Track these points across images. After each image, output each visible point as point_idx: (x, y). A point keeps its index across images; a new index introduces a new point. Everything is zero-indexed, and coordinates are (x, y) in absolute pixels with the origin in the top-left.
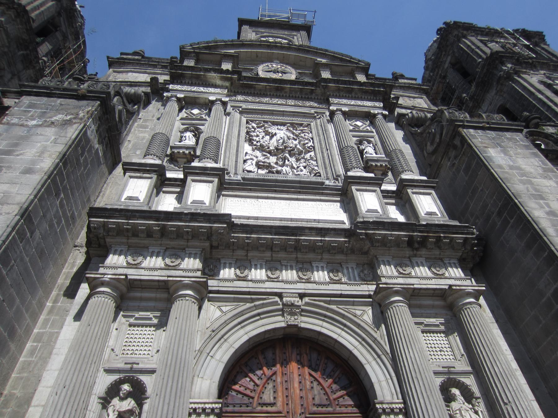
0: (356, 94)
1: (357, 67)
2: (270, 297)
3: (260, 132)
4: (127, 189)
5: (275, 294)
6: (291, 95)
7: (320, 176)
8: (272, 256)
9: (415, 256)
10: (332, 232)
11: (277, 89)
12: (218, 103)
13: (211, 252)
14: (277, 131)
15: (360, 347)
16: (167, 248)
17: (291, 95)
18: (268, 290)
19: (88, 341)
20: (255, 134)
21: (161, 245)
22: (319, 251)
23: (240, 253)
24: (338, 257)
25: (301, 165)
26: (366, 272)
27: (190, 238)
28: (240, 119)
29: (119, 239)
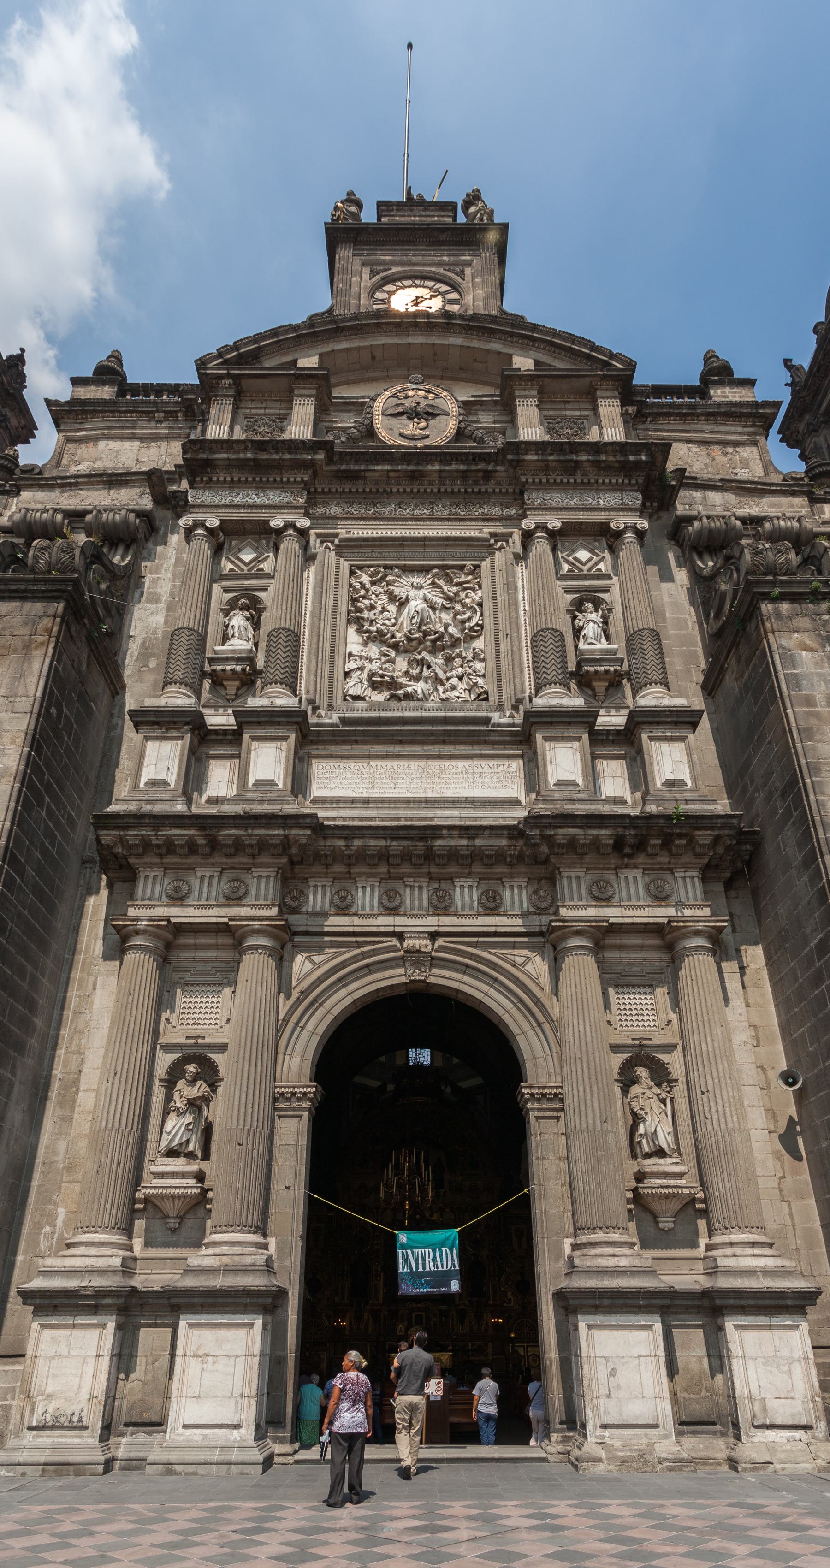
0: (585, 474)
1: (604, 377)
2: (385, 939)
3: (377, 596)
4: (145, 764)
5: (393, 934)
6: (442, 490)
7: (486, 699)
8: (389, 872)
9: (627, 866)
10: (487, 832)
11: (414, 477)
12: (290, 535)
13: (292, 870)
14: (412, 593)
15: (514, 1011)
16: (223, 869)
17: (442, 490)
18: (382, 929)
19: (134, 1014)
20: (367, 602)
21: (213, 865)
22: (465, 862)
23: (339, 868)
24: (497, 870)
25: (454, 673)
26: (542, 893)
27: (256, 851)
28: (338, 563)
29: (148, 859)
